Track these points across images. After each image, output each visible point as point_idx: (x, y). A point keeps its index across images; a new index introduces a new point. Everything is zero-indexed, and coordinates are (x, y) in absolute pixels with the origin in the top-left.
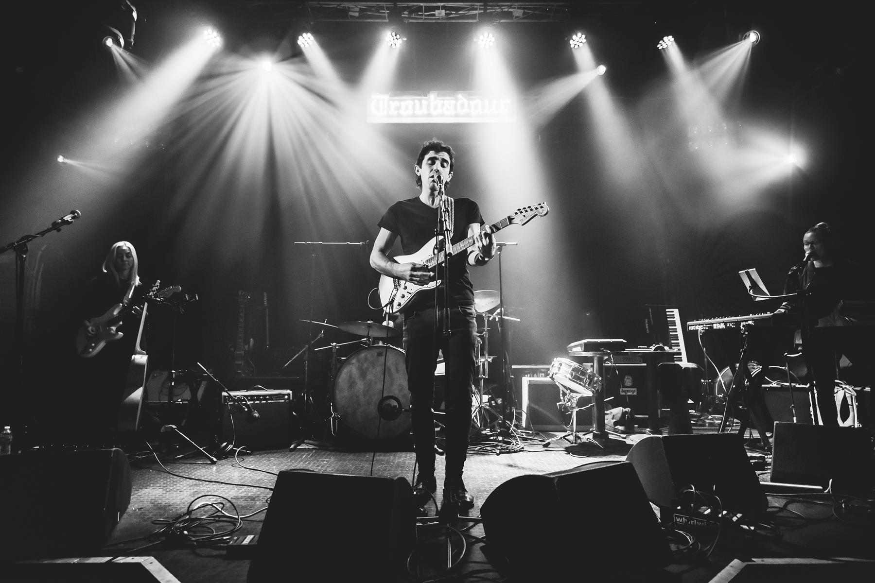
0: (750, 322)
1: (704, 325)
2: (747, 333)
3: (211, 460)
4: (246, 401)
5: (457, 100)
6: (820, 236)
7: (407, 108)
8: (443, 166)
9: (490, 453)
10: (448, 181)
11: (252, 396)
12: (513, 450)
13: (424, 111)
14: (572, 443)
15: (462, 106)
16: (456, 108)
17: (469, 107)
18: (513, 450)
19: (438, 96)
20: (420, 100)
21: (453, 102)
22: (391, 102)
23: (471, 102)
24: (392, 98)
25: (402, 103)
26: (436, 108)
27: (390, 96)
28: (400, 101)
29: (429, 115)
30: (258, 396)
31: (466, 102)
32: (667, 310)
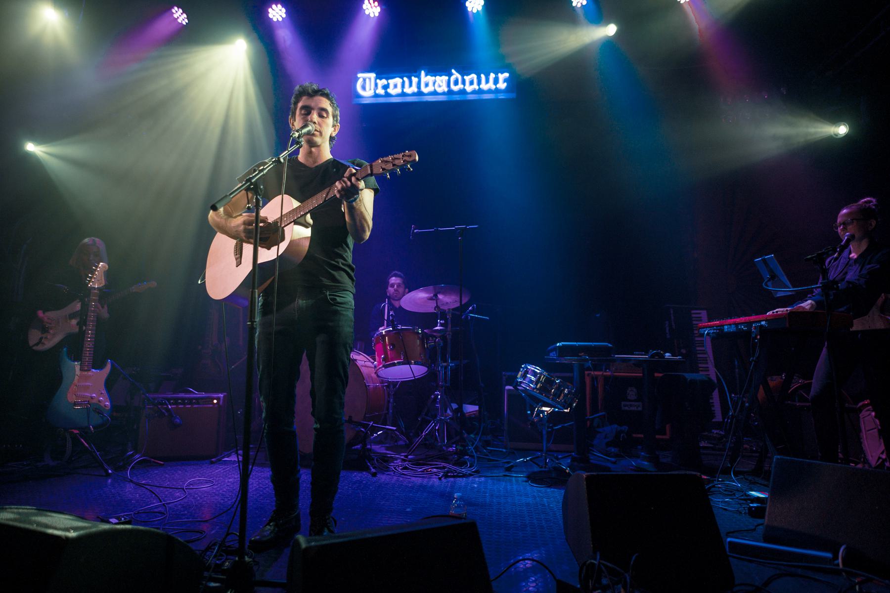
0: (763, 323)
1: (715, 328)
2: (759, 337)
3: (107, 471)
4: (167, 405)
5: (450, 75)
6: (865, 214)
7: (395, 86)
8: (321, 116)
9: (434, 476)
10: (334, 135)
11: (176, 399)
12: (462, 473)
13: (414, 89)
14: (542, 467)
15: (456, 83)
17: (464, 82)
18: (462, 473)
21: (445, 78)
22: (378, 81)
23: (465, 77)
24: (379, 76)
26: (427, 85)
27: (377, 74)
28: (387, 79)
29: (420, 93)
30: (183, 399)
31: (460, 77)
32: (693, 312)
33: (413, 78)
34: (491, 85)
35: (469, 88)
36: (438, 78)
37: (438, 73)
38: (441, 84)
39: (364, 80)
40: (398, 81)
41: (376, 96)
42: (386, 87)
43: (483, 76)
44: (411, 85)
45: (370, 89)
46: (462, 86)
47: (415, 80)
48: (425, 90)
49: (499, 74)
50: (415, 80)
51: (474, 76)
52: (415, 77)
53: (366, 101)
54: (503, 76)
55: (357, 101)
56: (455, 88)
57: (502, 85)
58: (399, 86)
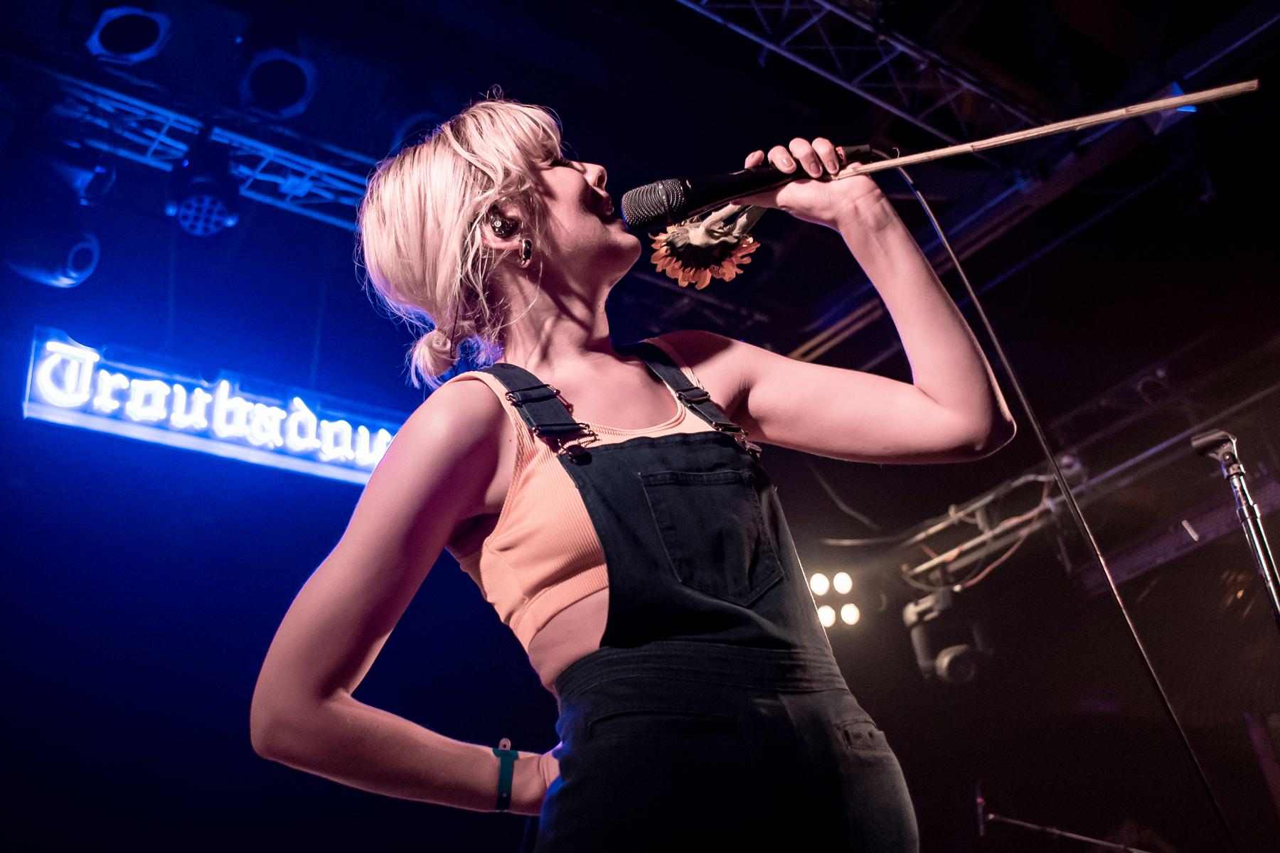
7: (148, 400)
15: (302, 431)
16: (283, 432)
17: (318, 436)
19: (242, 389)
20: (190, 389)
21: (277, 413)
22: (104, 373)
23: (324, 423)
25: (135, 382)
26: (230, 418)
27: (106, 356)
28: (131, 376)
29: (206, 434)
39: (64, 363)
40: (158, 388)
41: (86, 410)
42: (122, 395)
43: (363, 430)
44: (189, 406)
45: (77, 389)
47: (200, 396)
48: (222, 429)
51: (343, 426)
52: (206, 390)
55: (29, 411)
56: (297, 444)
58: (159, 401)
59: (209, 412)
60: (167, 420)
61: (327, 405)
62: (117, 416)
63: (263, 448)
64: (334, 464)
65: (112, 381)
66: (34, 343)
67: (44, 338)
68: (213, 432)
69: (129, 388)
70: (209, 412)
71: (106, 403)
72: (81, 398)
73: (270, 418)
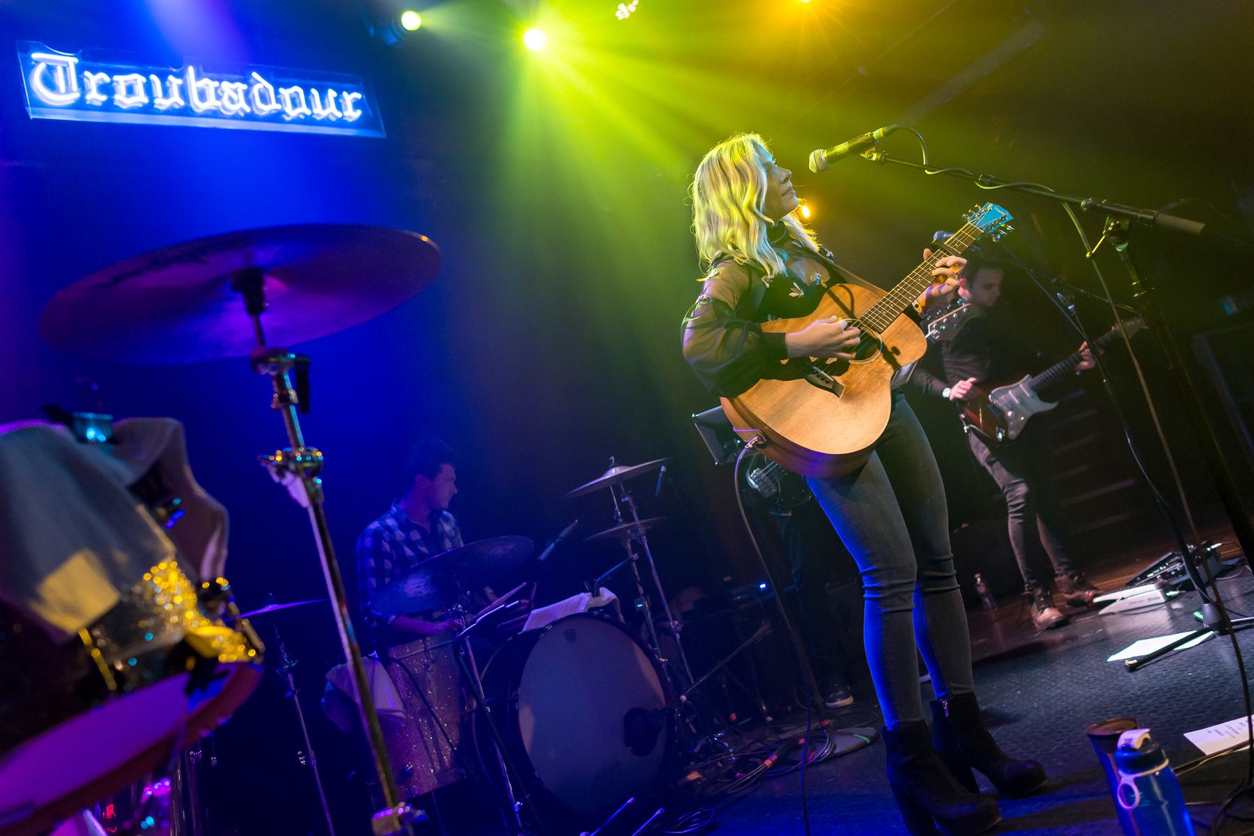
7: (130, 90)
13: (176, 100)
15: (264, 99)
17: (278, 101)
19: (206, 70)
20: (163, 78)
21: (242, 87)
22: (87, 73)
23: (281, 90)
24: (88, 63)
25: (116, 78)
26: (202, 95)
27: (83, 57)
28: (111, 73)
29: (186, 111)
31: (271, 88)
33: (171, 78)
34: (331, 111)
35: (292, 113)
36: (226, 85)
37: (224, 76)
38: (235, 97)
39: (51, 69)
40: (138, 80)
41: (80, 105)
42: (107, 89)
43: (314, 91)
44: (166, 93)
46: (279, 107)
47: (174, 82)
48: (199, 106)
49: (345, 94)
50: (174, 82)
52: (177, 76)
53: (51, 114)
54: (349, 98)
57: (353, 114)
58: (140, 89)
59: (184, 92)
60: (151, 104)
61: (280, 74)
62: (109, 106)
63: (235, 117)
64: (296, 121)
65: (94, 80)
66: (19, 55)
67: (27, 50)
68: (191, 108)
69: (112, 82)
70: (184, 92)
71: (95, 97)
72: (75, 95)
73: (236, 91)
